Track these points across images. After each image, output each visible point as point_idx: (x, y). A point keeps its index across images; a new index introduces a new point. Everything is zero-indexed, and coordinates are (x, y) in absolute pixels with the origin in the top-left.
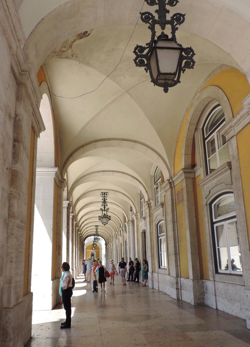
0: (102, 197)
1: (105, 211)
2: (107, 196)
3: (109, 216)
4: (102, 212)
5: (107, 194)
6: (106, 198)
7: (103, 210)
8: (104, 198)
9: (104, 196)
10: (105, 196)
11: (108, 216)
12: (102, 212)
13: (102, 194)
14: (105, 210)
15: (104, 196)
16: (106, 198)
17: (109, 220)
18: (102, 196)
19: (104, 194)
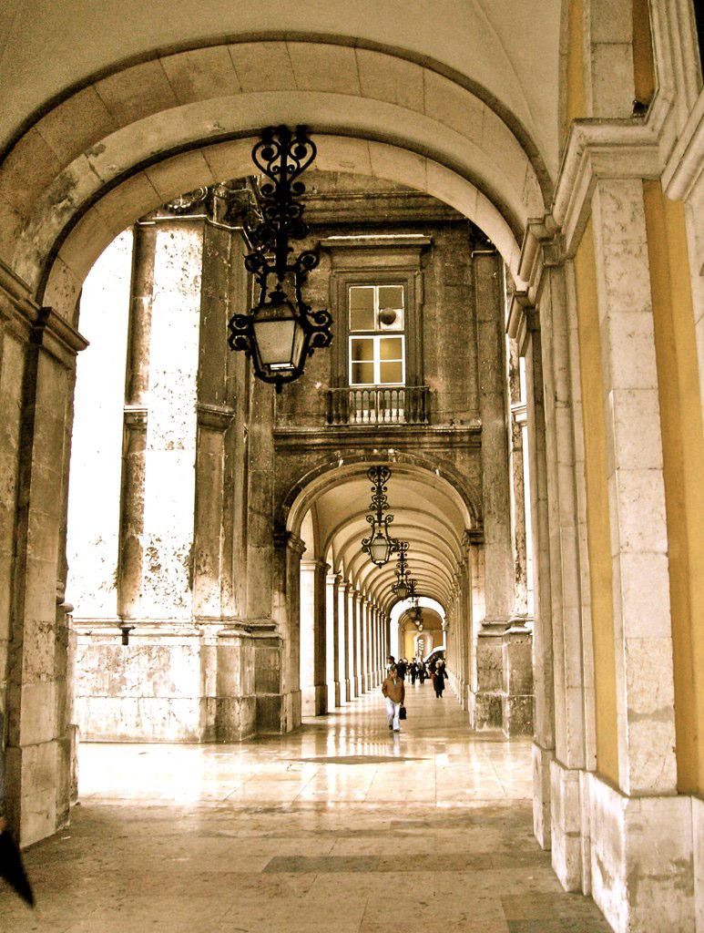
0: (267, 172)
1: (281, 278)
2: (303, 162)
3: (315, 310)
4: (262, 281)
5: (301, 153)
6: (297, 180)
7: (267, 270)
8: (277, 177)
9: (278, 163)
10: (290, 162)
11: (305, 308)
12: (262, 281)
13: (268, 155)
14: (281, 269)
15: (278, 163)
16: (297, 180)
17: (320, 342)
18: (264, 164)
19: (284, 152)
